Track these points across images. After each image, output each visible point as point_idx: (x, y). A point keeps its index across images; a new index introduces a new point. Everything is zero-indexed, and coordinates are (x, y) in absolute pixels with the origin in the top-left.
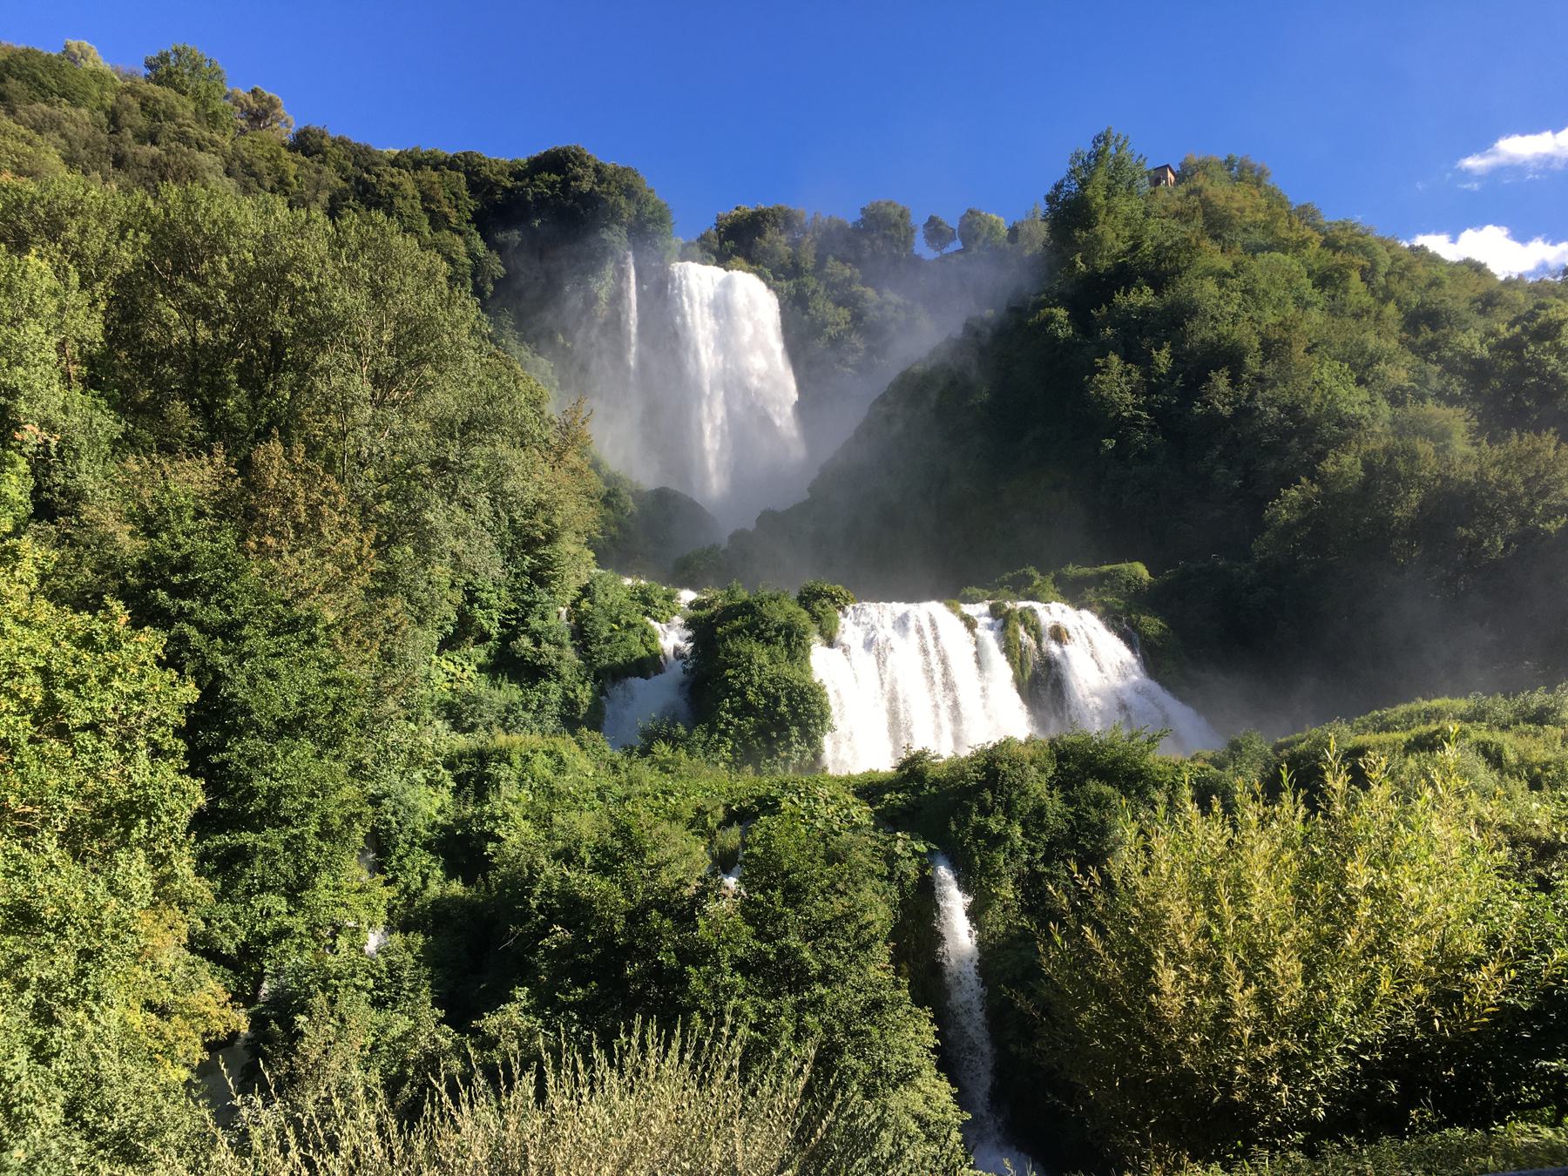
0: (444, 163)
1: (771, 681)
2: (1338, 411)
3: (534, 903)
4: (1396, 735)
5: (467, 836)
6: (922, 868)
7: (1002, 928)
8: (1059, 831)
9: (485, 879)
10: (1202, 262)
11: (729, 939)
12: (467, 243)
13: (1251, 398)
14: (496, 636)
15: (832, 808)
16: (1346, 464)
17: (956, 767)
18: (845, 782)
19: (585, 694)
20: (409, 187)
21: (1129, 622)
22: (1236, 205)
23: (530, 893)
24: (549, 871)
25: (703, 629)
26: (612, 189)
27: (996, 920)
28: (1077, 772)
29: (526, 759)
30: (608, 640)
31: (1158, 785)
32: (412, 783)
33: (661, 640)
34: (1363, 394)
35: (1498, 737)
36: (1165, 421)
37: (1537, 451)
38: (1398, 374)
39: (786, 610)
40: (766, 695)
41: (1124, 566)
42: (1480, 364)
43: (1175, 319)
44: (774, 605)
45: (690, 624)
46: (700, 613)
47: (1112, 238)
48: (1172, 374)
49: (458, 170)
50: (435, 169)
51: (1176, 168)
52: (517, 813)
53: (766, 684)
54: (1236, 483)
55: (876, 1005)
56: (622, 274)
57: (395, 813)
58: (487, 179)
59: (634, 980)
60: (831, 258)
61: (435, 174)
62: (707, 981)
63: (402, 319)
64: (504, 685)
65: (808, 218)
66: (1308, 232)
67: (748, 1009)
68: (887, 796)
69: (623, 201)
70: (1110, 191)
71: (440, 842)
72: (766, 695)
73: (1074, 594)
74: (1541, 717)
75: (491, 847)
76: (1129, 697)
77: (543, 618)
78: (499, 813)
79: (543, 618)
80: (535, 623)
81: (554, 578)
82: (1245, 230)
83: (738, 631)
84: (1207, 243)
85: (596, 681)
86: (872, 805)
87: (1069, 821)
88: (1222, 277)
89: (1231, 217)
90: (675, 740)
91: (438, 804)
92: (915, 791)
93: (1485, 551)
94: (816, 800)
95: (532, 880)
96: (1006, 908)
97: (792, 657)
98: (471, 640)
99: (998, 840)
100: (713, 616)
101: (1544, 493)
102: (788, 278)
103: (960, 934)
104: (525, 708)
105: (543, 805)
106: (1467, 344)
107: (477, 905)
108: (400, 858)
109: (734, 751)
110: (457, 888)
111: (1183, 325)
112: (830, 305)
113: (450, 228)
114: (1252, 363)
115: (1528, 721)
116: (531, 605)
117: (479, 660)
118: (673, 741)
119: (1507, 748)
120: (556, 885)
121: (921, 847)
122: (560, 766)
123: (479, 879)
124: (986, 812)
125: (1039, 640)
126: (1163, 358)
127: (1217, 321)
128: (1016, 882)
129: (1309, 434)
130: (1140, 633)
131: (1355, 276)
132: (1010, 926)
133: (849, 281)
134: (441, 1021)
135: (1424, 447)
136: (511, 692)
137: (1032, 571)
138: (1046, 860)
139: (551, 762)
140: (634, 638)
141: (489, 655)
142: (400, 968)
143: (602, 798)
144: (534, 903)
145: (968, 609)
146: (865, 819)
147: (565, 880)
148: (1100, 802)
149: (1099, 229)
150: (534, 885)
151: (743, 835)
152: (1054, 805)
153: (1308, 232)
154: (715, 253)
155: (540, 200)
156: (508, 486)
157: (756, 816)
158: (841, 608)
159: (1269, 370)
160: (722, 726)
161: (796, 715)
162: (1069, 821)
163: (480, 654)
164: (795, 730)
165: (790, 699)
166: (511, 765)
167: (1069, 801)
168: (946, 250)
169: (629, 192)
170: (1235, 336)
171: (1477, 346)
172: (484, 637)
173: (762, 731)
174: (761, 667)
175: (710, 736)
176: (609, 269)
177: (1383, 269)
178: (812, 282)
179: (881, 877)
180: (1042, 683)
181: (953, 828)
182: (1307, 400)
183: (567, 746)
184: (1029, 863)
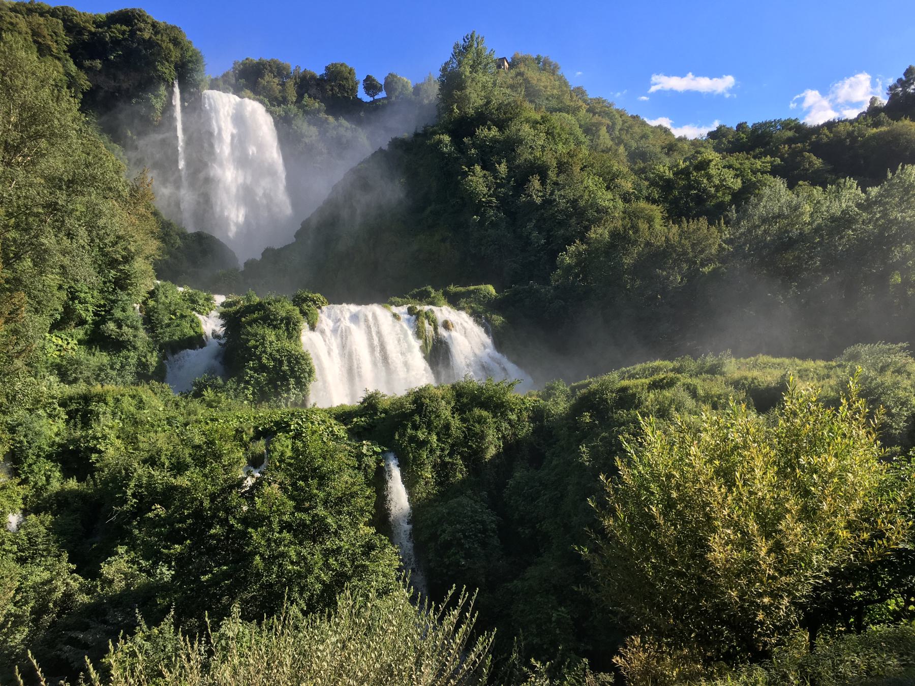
1: (278, 351)
2: (597, 204)
3: (129, 492)
4: (643, 380)
5: (77, 451)
6: (378, 462)
7: (424, 495)
8: (458, 438)
9: (93, 477)
10: (525, 114)
11: (278, 510)
12: (64, 66)
13: (552, 194)
14: (90, 321)
15: (322, 427)
16: (600, 233)
17: (398, 404)
18: (329, 412)
19: (153, 359)
20: (22, 25)
21: (486, 318)
22: (542, 84)
23: (127, 486)
24: (140, 471)
25: (233, 319)
26: (164, 38)
27: (421, 490)
28: (467, 404)
29: (118, 400)
30: (168, 325)
31: (512, 410)
32: (39, 416)
33: (204, 327)
34: (609, 195)
35: (695, 381)
36: (505, 204)
37: (699, 229)
38: (627, 185)
39: (285, 308)
40: (274, 360)
41: (482, 287)
42: (668, 181)
43: (509, 147)
44: (278, 305)
45: (223, 316)
46: (230, 309)
47: (475, 98)
48: (509, 178)
49: (57, 17)
50: (41, 15)
51: (509, 60)
52: (112, 435)
53: (275, 352)
54: (543, 241)
55: (369, 547)
56: (171, 93)
57: (25, 436)
58: (78, 24)
59: (213, 537)
60: (306, 95)
61: (42, 19)
62: (263, 536)
63: (23, 107)
64: (97, 353)
65: (292, 69)
66: (580, 103)
67: (292, 553)
68: (355, 420)
69: (171, 46)
70: (474, 68)
71: (58, 454)
72: (274, 360)
73: (454, 301)
74: (714, 370)
75: (94, 457)
76: (486, 359)
77: (124, 310)
78: (99, 435)
79: (124, 310)
80: (118, 314)
81: (131, 285)
82: (547, 99)
83: (255, 321)
84: (527, 104)
85: (160, 351)
86: (346, 425)
87: (464, 432)
88: (535, 124)
89: (540, 90)
90: (216, 387)
91: (56, 430)
92: (371, 416)
93: (672, 282)
94: (312, 423)
95: (128, 477)
96: (427, 483)
97: (290, 337)
98: (73, 324)
99: (423, 444)
100: (238, 312)
101: (702, 251)
102: (279, 105)
103: (399, 498)
104: (112, 368)
105: (130, 429)
106: (662, 170)
107: (86, 494)
108: (30, 465)
109: (253, 394)
110: (72, 484)
111: (514, 150)
113: (52, 55)
114: (552, 174)
115: (707, 372)
116: (114, 302)
117: (79, 337)
118: (215, 387)
119: (699, 388)
120: (145, 480)
121: (378, 449)
122: (141, 405)
123: (89, 477)
124: (416, 427)
125: (436, 329)
126: (503, 168)
127: (533, 149)
128: (434, 467)
129: (582, 216)
130: (492, 325)
131: (603, 130)
132: (429, 493)
133: (319, 111)
134: (72, 572)
135: (643, 226)
136: (102, 358)
137: (430, 288)
138: (450, 455)
139: (134, 402)
140: (186, 324)
141: (86, 334)
142: (37, 536)
143: (170, 424)
144: (129, 492)
145: (394, 309)
146: (342, 434)
147: (151, 476)
148: (481, 420)
149: (468, 91)
150: (130, 480)
151: (267, 445)
152: (456, 423)
153: (580, 103)
154: (232, 85)
155: (116, 42)
156: (101, 222)
157: (275, 433)
158: (320, 308)
159: (562, 179)
160: (247, 378)
161: (292, 372)
162: (464, 432)
163: (80, 333)
164: (292, 381)
165: (289, 362)
166: (106, 404)
167: (463, 420)
168: (376, 97)
169: (176, 42)
170: (544, 159)
171: (667, 172)
172: (82, 322)
173: (271, 381)
174: (271, 343)
175: (238, 385)
176: (162, 90)
177: (618, 127)
178: (293, 108)
179: (354, 468)
180: (438, 352)
181: (397, 437)
182: (581, 197)
183: (144, 391)
184: (440, 457)
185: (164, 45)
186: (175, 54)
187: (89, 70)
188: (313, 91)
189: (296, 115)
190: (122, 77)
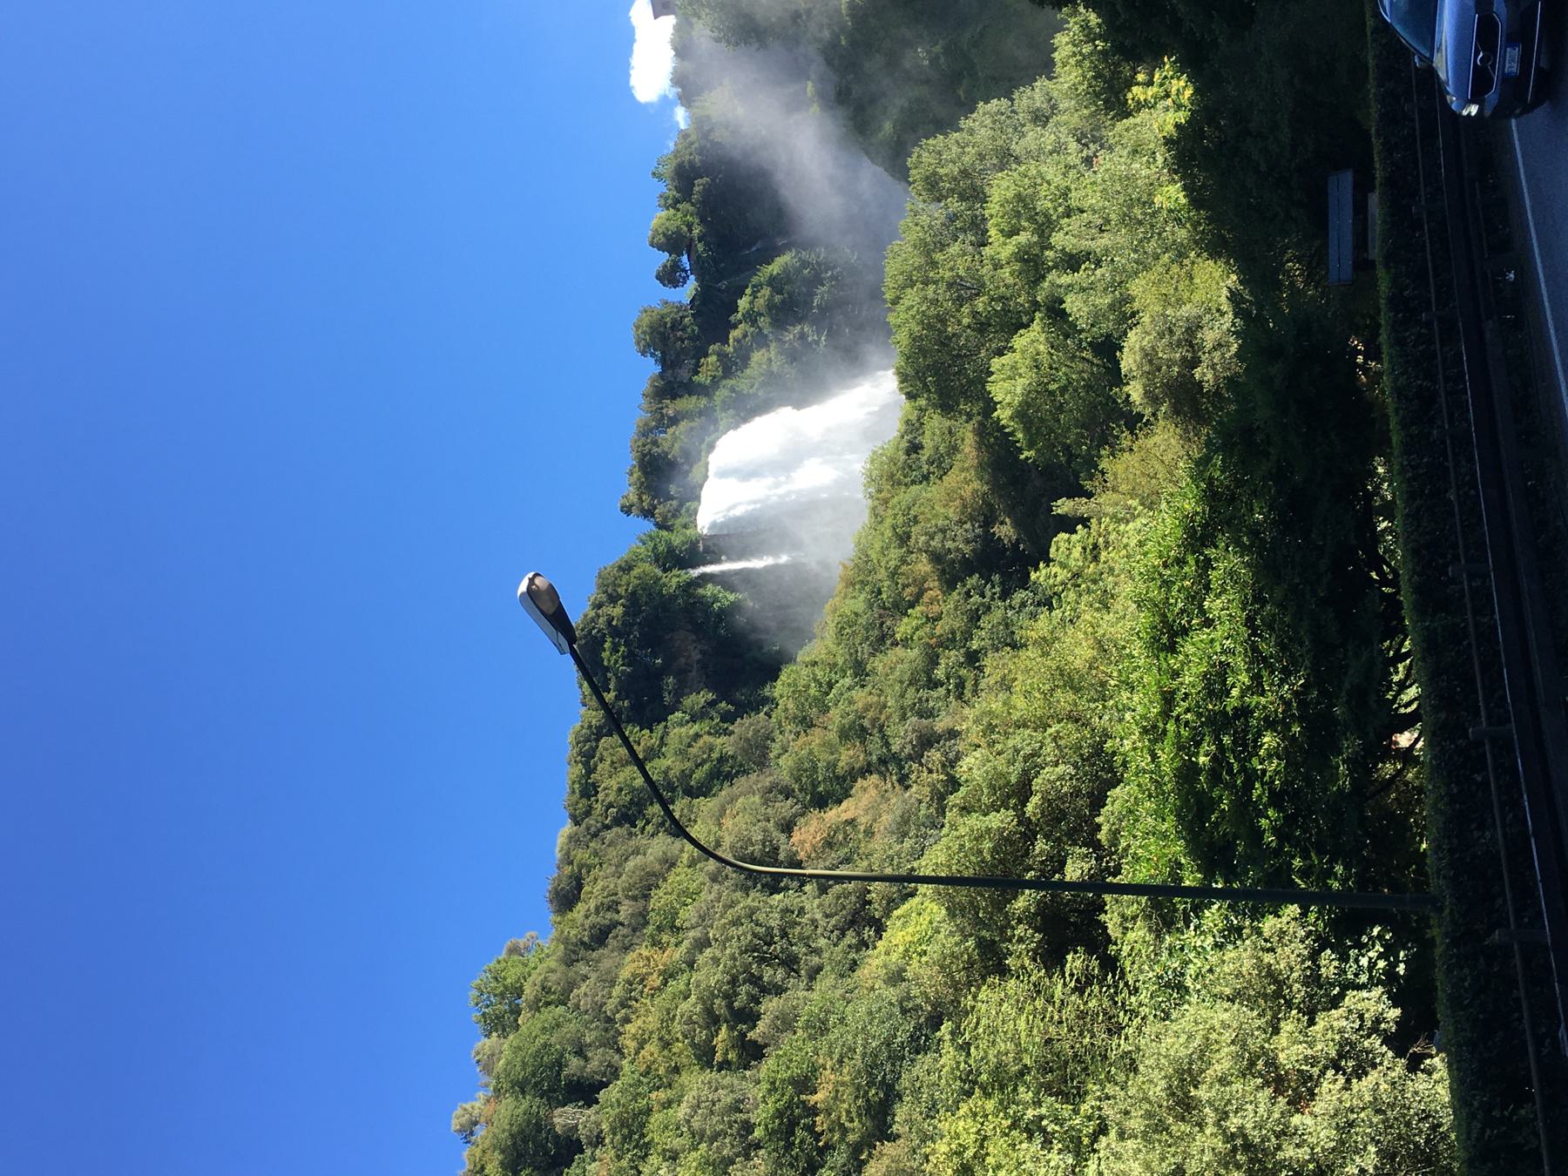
0: (586, 764)
56: (705, 578)
69: (635, 572)
112: (748, 371)
133: (722, 356)
155: (630, 658)
169: (626, 568)
176: (709, 590)
185: (637, 582)
186: (648, 568)
187: (679, 694)
188: (684, 374)
189: (733, 390)
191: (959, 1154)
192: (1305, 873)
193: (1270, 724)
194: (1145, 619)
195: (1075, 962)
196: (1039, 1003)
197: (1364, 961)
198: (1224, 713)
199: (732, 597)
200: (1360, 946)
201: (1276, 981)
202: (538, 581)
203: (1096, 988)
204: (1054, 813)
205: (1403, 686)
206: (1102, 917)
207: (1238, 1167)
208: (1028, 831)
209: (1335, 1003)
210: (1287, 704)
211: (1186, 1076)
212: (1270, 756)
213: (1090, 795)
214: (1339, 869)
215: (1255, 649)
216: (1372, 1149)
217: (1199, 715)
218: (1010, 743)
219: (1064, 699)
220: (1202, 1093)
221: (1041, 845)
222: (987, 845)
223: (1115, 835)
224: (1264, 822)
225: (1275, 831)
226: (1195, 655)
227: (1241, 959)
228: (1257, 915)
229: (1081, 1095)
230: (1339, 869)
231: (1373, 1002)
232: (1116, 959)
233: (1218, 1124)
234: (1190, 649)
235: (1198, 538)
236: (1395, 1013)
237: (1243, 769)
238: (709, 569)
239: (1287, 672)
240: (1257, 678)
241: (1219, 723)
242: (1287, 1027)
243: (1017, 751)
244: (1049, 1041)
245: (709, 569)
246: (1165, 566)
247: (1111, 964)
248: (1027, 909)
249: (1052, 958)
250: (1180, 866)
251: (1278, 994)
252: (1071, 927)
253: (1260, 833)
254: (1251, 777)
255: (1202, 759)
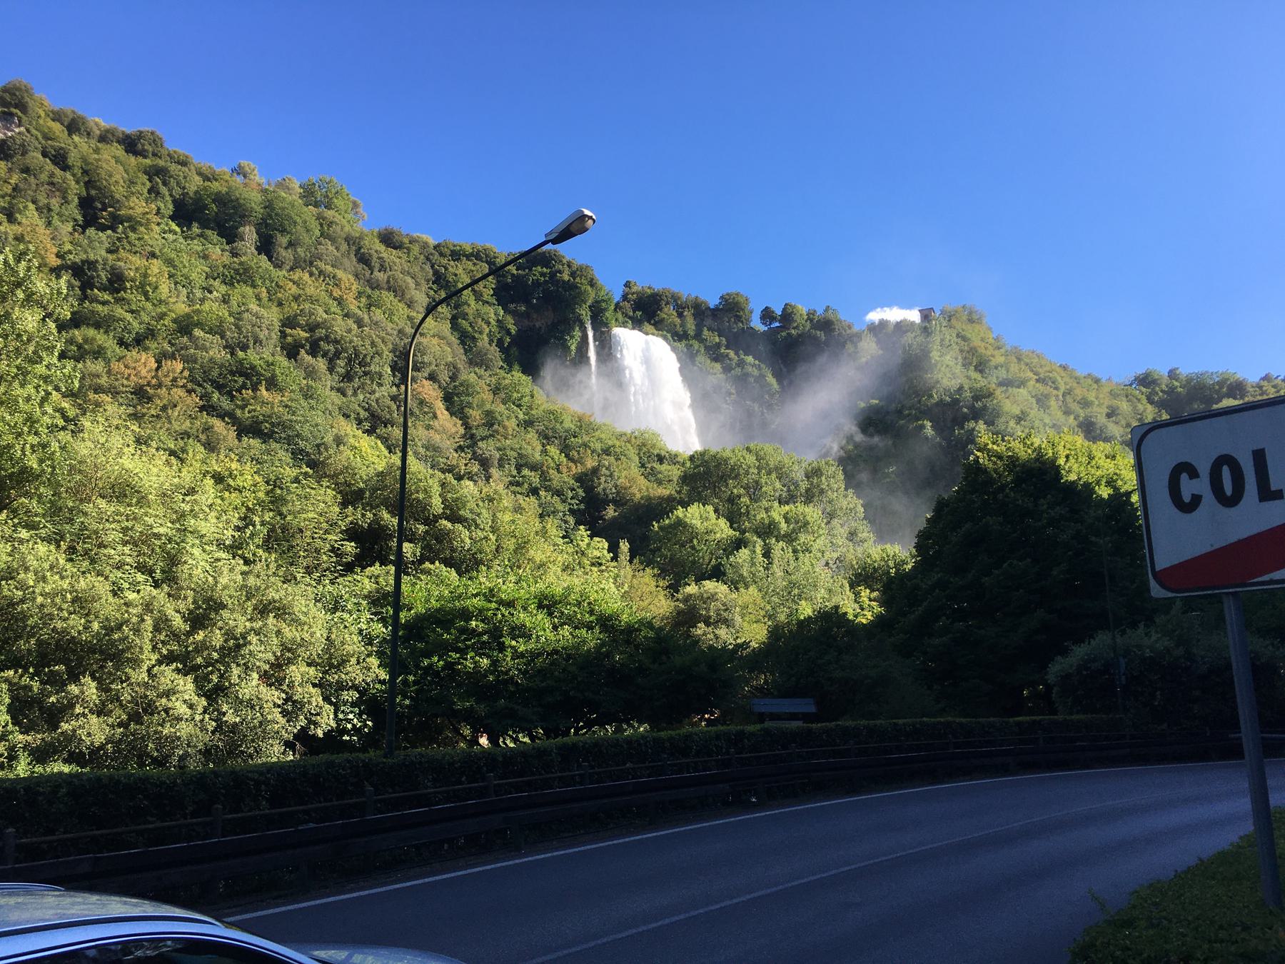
0: (472, 254)
102: (680, 340)
133: (718, 345)
155: (536, 284)
169: (592, 283)
176: (577, 333)
178: (696, 345)
186: (591, 296)
187: (514, 313)
189: (698, 351)
190: (535, 316)
191: (231, 475)
192: (405, 682)
193: (495, 663)
194: (558, 590)
195: (350, 547)
196: (325, 525)
197: (351, 716)
198: (502, 636)
199: (573, 347)
200: (360, 714)
201: (339, 665)
202: (590, 222)
203: (334, 559)
204: (442, 537)
205: (515, 740)
206: (377, 564)
207: (226, 641)
208: (430, 521)
209: (326, 699)
210: (507, 673)
211: (282, 611)
212: (475, 663)
213: (452, 557)
214: (407, 702)
215: (540, 654)
216: (238, 720)
217: (500, 622)
218: (484, 511)
219: (510, 544)
220: (271, 620)
221: (422, 528)
222: (421, 496)
223: (428, 572)
224: (436, 659)
225: (431, 665)
226: (538, 621)
227: (353, 644)
228: (380, 654)
229: (268, 550)
230: (407, 702)
231: (327, 721)
232: (352, 571)
233: (252, 629)
234: (540, 617)
235: (606, 622)
236: (320, 733)
237: (467, 647)
238: (590, 334)
239: (525, 673)
240: (522, 655)
241: (496, 633)
242: (312, 671)
243: (478, 515)
244: (301, 531)
245: (590, 334)
246: (589, 604)
247: (349, 568)
248: (382, 519)
249: (352, 533)
250: (409, 610)
251: (331, 666)
252: (370, 546)
253: (429, 656)
254: (463, 652)
255: (474, 623)
